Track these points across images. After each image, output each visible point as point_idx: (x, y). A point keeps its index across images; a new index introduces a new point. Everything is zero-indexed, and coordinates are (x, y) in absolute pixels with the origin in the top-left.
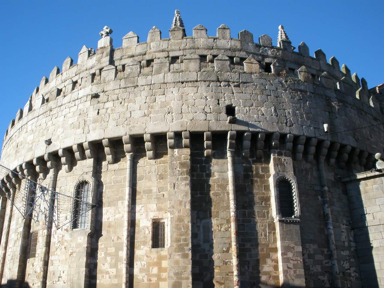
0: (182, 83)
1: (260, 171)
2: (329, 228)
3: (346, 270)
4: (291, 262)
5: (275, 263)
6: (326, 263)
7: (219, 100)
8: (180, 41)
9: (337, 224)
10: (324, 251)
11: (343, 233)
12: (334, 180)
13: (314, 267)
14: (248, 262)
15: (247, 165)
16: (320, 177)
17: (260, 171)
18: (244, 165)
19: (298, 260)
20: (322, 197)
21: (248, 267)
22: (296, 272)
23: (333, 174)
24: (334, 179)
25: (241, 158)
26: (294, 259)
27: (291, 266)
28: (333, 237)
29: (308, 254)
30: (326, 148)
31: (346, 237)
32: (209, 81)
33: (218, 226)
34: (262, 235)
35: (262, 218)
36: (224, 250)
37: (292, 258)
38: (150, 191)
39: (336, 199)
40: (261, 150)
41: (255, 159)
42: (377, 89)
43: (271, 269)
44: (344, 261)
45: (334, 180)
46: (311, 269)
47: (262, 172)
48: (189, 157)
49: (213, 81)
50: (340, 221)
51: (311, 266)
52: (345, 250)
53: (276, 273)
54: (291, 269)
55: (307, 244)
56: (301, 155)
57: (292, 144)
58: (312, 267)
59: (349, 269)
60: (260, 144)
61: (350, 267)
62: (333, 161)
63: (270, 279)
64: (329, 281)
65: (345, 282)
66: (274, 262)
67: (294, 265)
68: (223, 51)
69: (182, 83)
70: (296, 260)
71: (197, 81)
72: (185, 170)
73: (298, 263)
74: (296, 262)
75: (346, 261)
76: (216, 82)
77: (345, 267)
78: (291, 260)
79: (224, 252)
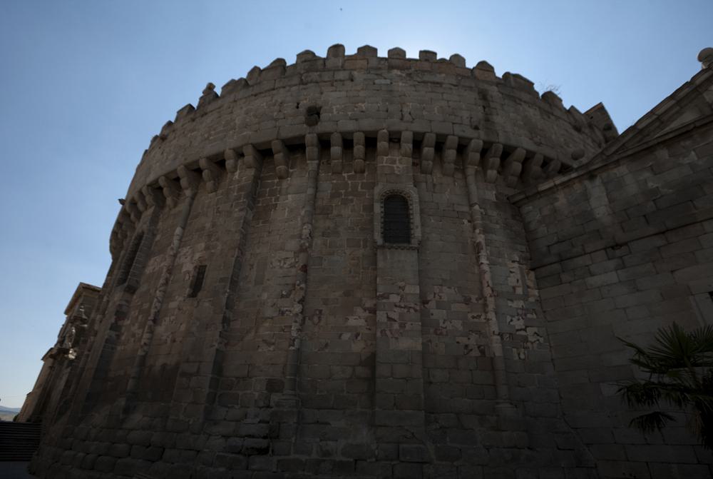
1: (359, 188)
2: (482, 263)
3: (518, 330)
4: (396, 309)
5: (370, 313)
6: (473, 317)
9: (500, 260)
10: (470, 299)
11: (512, 275)
12: (495, 200)
13: (447, 323)
14: (321, 311)
15: (339, 182)
16: (468, 195)
17: (359, 188)
18: (335, 182)
19: (410, 307)
20: (469, 221)
21: (319, 318)
22: (405, 327)
23: (494, 192)
25: (330, 174)
26: (403, 306)
27: (395, 316)
28: (487, 277)
29: (437, 302)
30: (476, 152)
31: (518, 281)
33: (280, 261)
36: (282, 295)
37: (398, 304)
38: (203, 228)
40: (361, 159)
41: (353, 173)
43: (362, 322)
44: (513, 316)
45: (495, 200)
46: (441, 324)
47: (362, 188)
48: (252, 178)
50: (506, 256)
51: (441, 321)
52: (516, 300)
53: (370, 329)
54: (395, 321)
55: (436, 287)
56: (431, 162)
57: (411, 146)
58: (444, 323)
59: (525, 330)
60: (359, 149)
61: (527, 327)
62: (492, 173)
63: (357, 338)
64: (479, 347)
65: (514, 350)
66: (367, 312)
67: (401, 315)
70: (405, 307)
73: (408, 311)
74: (406, 310)
75: (517, 317)
77: (514, 326)
78: (396, 306)
79: (282, 296)
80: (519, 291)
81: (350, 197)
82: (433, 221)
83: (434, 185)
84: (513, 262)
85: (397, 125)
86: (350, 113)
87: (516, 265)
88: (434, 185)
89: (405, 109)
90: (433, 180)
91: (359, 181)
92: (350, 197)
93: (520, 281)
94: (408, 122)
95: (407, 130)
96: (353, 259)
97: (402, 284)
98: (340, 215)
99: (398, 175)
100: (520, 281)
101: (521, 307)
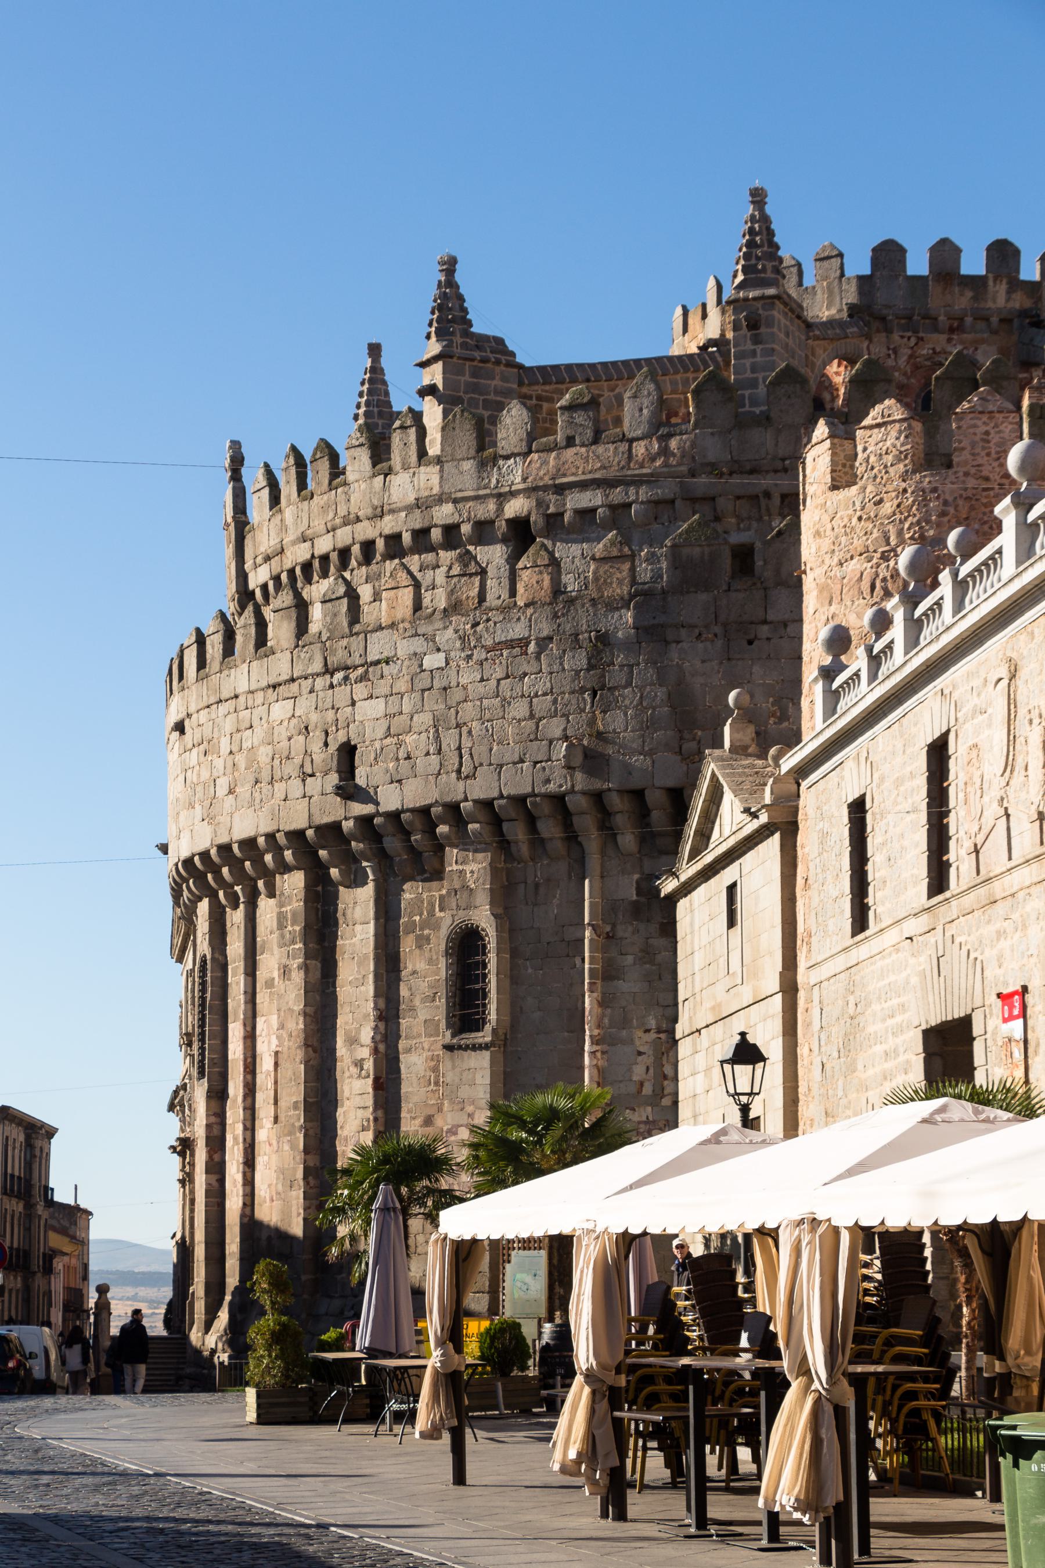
0: (274, 687)
1: (437, 909)
7: (327, 734)
8: (325, 497)
9: (624, 1033)
11: (640, 1058)
12: (635, 898)
23: (636, 876)
24: (637, 895)
31: (648, 1069)
32: (313, 675)
34: (430, 1084)
35: (432, 1039)
39: (630, 959)
42: (196, 859)
49: (318, 675)
52: (639, 1107)
68: (403, 514)
69: (274, 687)
71: (293, 680)
72: (297, 928)
76: (324, 674)
80: (648, 1089)
81: (426, 932)
82: (530, 971)
83: (537, 886)
84: (647, 1031)
85: (456, 790)
86: (391, 765)
87: (655, 1036)
88: (537, 886)
89: (466, 743)
90: (536, 876)
91: (437, 894)
92: (426, 932)
93: (651, 1071)
94: (467, 777)
95: (466, 799)
96: (432, 1060)
97: (470, 1109)
98: (414, 972)
99: (471, 890)
100: (651, 1071)
101: (644, 1119)
